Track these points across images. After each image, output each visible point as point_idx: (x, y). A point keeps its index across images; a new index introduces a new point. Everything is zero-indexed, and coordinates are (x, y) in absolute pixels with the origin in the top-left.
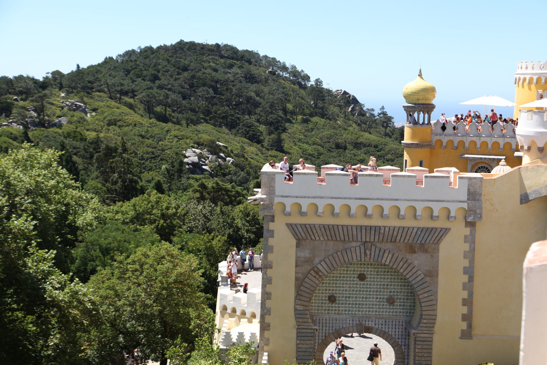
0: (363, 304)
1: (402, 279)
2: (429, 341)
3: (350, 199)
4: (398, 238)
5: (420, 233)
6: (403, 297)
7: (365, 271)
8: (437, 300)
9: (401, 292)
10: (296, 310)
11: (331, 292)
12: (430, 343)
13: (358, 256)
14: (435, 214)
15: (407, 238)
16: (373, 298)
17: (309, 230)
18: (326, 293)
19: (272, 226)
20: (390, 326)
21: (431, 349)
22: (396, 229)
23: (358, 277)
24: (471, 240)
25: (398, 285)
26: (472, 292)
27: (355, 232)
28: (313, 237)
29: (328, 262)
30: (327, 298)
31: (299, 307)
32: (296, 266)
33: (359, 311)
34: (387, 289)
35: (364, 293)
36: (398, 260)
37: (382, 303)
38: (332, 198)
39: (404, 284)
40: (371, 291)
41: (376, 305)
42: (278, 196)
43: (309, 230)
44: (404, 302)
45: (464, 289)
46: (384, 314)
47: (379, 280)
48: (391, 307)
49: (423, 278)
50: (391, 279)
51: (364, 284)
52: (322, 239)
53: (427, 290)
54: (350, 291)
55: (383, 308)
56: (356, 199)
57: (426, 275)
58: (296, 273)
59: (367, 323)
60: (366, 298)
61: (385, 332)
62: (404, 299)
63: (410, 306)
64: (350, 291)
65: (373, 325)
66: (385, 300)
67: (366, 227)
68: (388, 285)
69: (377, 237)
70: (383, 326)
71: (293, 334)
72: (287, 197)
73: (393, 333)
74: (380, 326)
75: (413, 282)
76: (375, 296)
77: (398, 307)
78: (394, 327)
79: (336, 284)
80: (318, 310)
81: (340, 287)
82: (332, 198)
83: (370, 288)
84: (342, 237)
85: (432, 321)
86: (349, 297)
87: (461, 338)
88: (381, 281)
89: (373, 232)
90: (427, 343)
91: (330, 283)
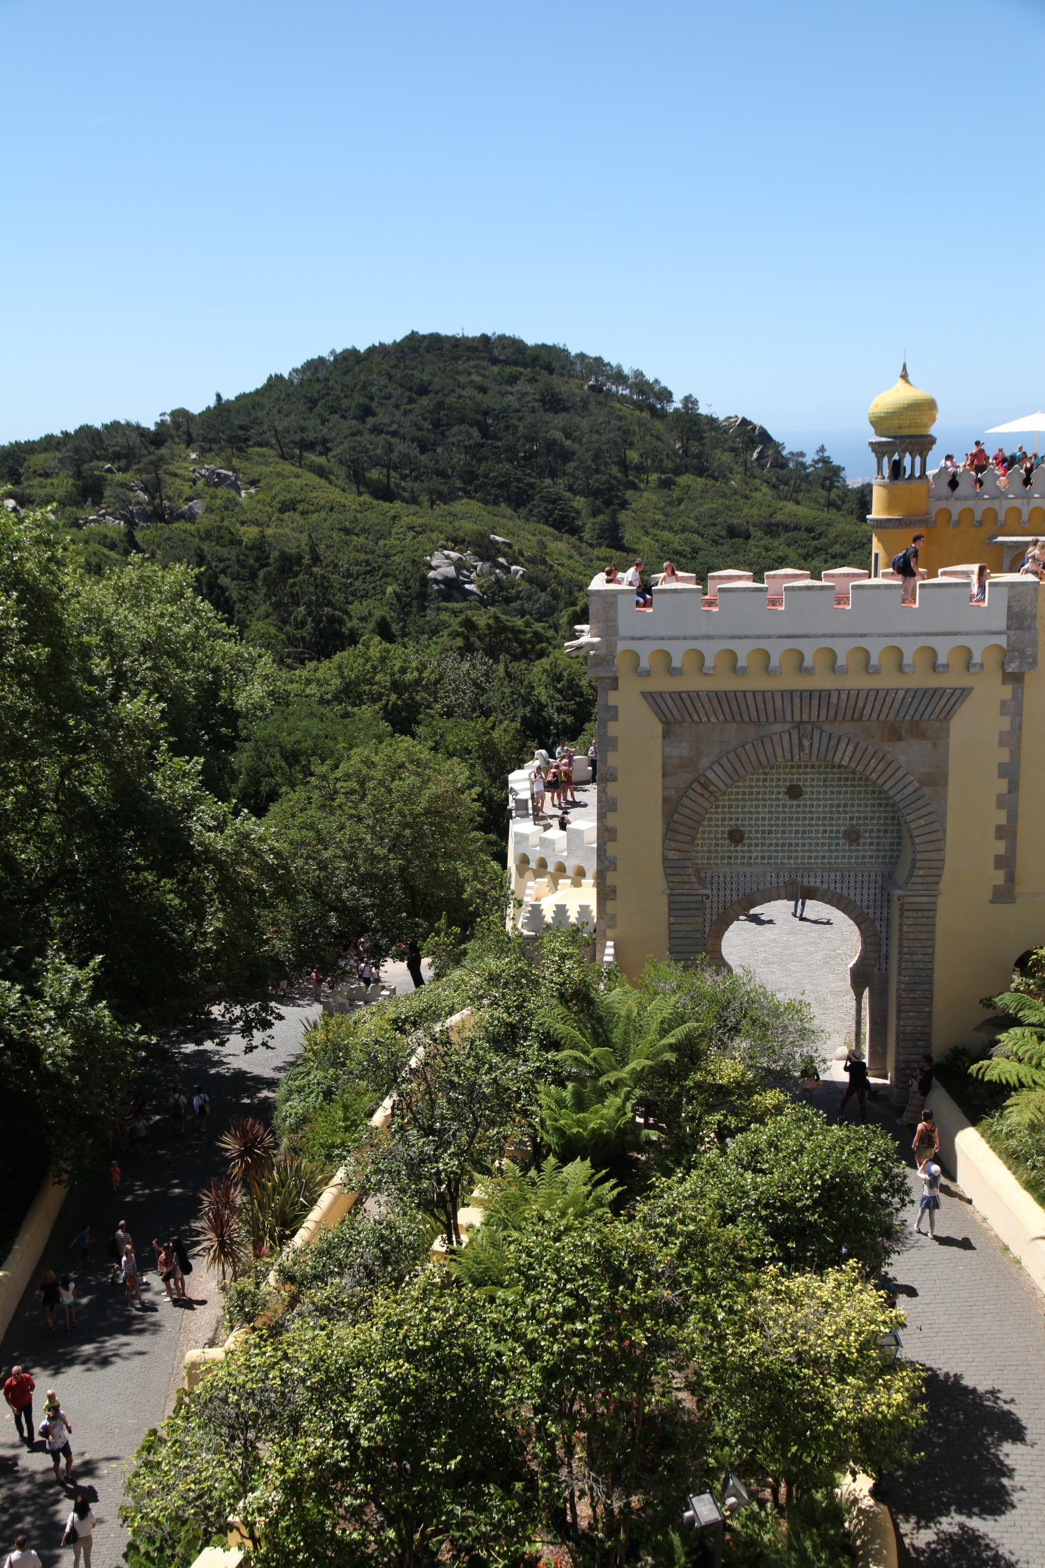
0: (797, 845)
1: (874, 792)
2: (931, 910)
3: (769, 637)
4: (867, 711)
8: (944, 830)
9: (872, 818)
10: (665, 859)
12: (931, 914)
14: (942, 660)
15: (885, 710)
16: (817, 832)
17: (688, 702)
19: (613, 698)
20: (852, 884)
21: (934, 925)
22: (862, 695)
23: (786, 793)
24: (1014, 709)
25: (866, 805)
26: (1016, 813)
27: (779, 704)
28: (696, 718)
29: (727, 765)
31: (671, 855)
32: (664, 776)
33: (790, 858)
34: (845, 812)
36: (867, 756)
38: (733, 637)
41: (824, 844)
42: (625, 638)
43: (688, 702)
44: (878, 837)
45: (999, 806)
50: (853, 793)
51: (798, 806)
52: (713, 719)
53: (924, 811)
54: (771, 819)
55: (837, 851)
56: (780, 637)
57: (922, 784)
58: (664, 788)
59: (806, 880)
60: (804, 832)
61: (842, 896)
62: (879, 831)
63: (892, 844)
64: (771, 819)
65: (818, 884)
67: (801, 692)
68: (846, 805)
69: (823, 712)
70: (839, 885)
71: (662, 905)
72: (642, 639)
73: (858, 897)
74: (832, 886)
75: (897, 798)
78: (859, 885)
79: (744, 806)
80: (709, 858)
81: (751, 813)
82: (733, 637)
83: (811, 812)
84: (754, 715)
85: (935, 872)
87: (992, 902)
88: (832, 799)
89: (815, 702)
90: (926, 914)
91: (730, 807)
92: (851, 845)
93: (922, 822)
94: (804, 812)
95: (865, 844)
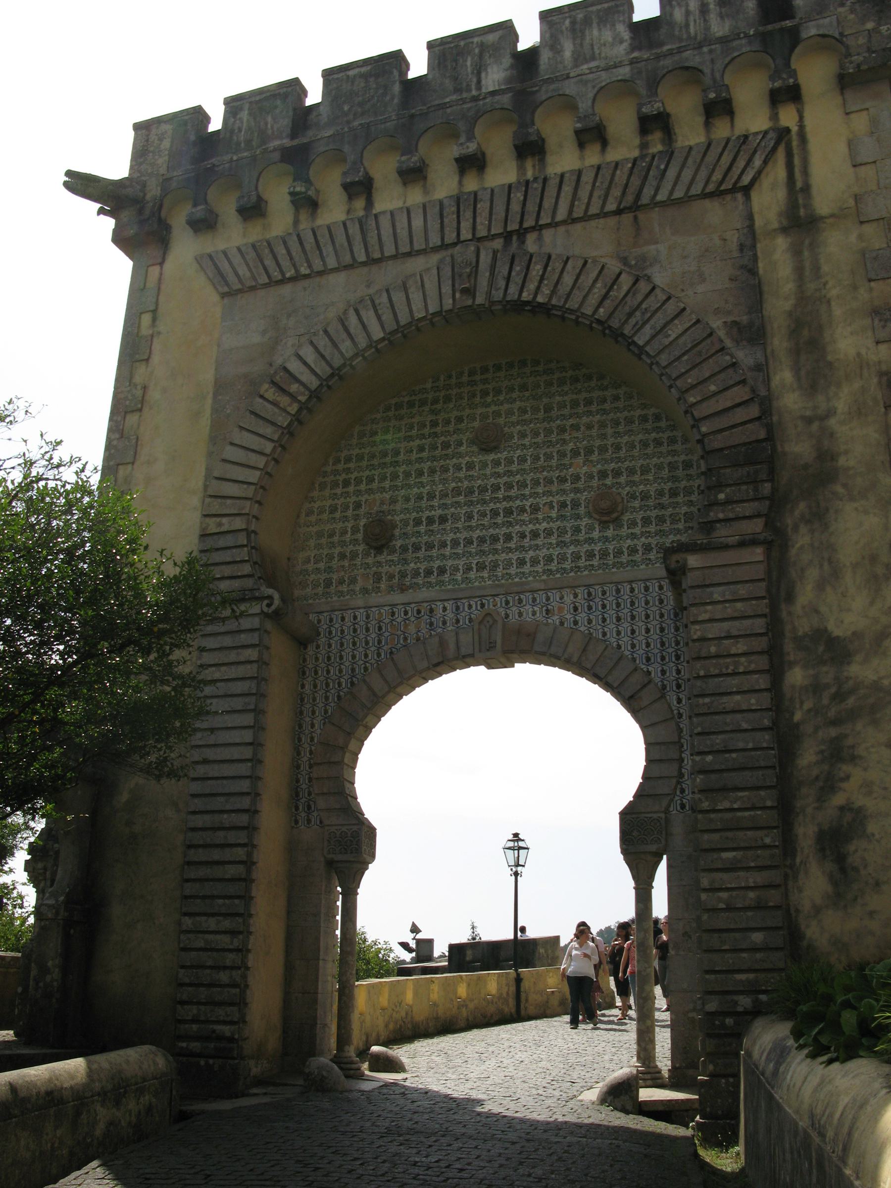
7: (500, 415)
20: (611, 613)
23: (472, 442)
30: (360, 536)
33: (481, 567)
39: (654, 435)
41: (549, 533)
48: (610, 533)
51: (497, 463)
54: (444, 495)
60: (508, 512)
62: (661, 493)
66: (582, 510)
70: (582, 617)
73: (625, 640)
78: (625, 612)
86: (443, 519)
92: (604, 525)
95: (633, 524)
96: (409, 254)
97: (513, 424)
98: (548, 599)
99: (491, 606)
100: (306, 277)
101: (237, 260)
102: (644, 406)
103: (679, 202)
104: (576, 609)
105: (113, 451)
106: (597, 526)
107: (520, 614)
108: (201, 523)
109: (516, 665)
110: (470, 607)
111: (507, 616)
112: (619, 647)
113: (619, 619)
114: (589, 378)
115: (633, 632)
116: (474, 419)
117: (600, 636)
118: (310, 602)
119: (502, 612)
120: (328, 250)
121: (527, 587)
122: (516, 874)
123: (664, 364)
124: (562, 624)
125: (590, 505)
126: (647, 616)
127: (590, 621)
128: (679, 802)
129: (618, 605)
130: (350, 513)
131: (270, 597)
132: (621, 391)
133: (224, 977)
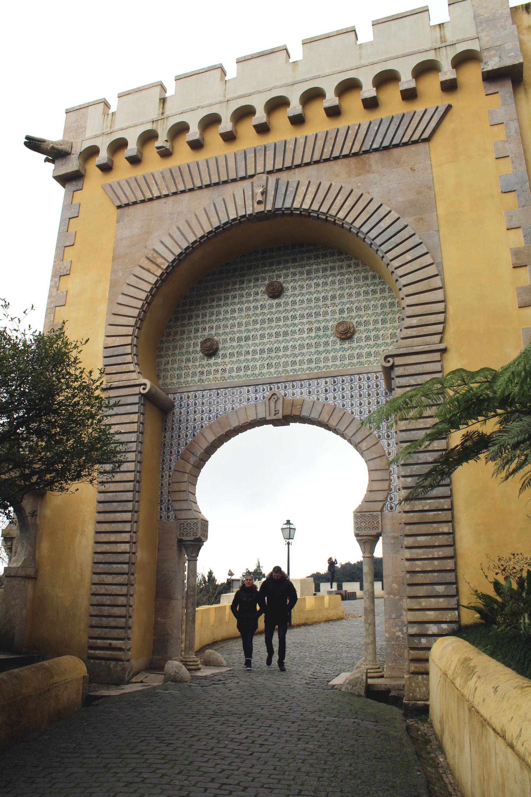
0: (278, 349)
5: (376, 128)
6: (373, 317)
8: (440, 265)
9: (366, 308)
11: (206, 333)
13: (238, 207)
15: (348, 144)
16: (301, 331)
18: (196, 337)
20: (347, 393)
23: (264, 293)
30: (198, 349)
34: (334, 305)
35: (281, 323)
37: (324, 340)
40: (294, 317)
41: (309, 346)
46: (330, 364)
47: (312, 290)
48: (346, 345)
49: (399, 218)
50: (341, 282)
51: (279, 305)
54: (247, 324)
60: (286, 334)
62: (376, 322)
65: (305, 396)
68: (333, 297)
70: (330, 395)
73: (356, 409)
74: (322, 396)
76: (307, 326)
77: (363, 344)
89: (270, 153)
93: (408, 257)
94: (286, 311)
95: (359, 340)
96: (225, 182)
97: (289, 283)
98: (310, 385)
99: (276, 389)
100: (166, 196)
101: (126, 187)
102: (366, 271)
103: (387, 148)
104: (326, 391)
105: (53, 299)
106: (338, 341)
107: (293, 394)
108: (104, 341)
109: (291, 424)
110: (264, 390)
111: (285, 395)
112: (352, 413)
113: (352, 396)
114: (333, 254)
115: (361, 404)
116: (265, 279)
117: (341, 407)
118: (169, 387)
119: (282, 392)
120: (179, 180)
121: (298, 378)
122: (289, 544)
123: (379, 244)
124: (318, 399)
125: (334, 329)
126: (369, 395)
127: (335, 398)
128: (389, 505)
129: (352, 388)
130: (192, 335)
131: (145, 384)
132: (352, 262)
133: (116, 611)
